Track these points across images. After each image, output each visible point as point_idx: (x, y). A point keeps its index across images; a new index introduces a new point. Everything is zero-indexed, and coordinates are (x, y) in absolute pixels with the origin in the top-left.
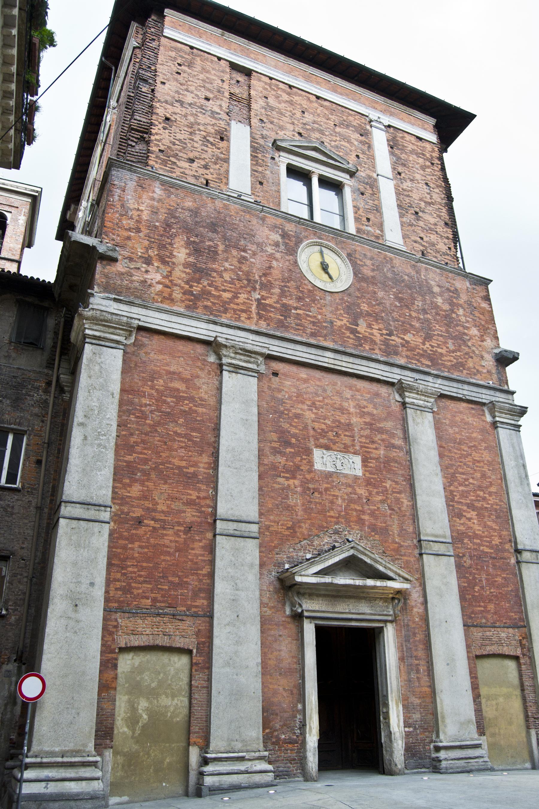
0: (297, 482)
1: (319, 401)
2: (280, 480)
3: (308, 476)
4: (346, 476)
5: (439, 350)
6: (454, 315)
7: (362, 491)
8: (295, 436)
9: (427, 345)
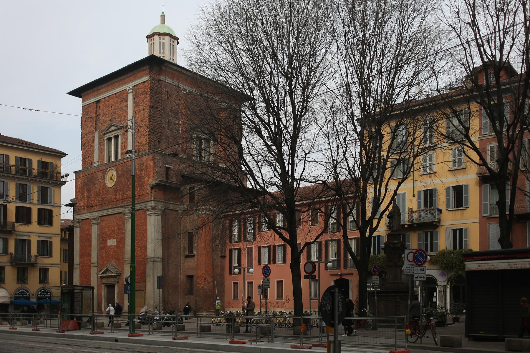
7: (115, 249)
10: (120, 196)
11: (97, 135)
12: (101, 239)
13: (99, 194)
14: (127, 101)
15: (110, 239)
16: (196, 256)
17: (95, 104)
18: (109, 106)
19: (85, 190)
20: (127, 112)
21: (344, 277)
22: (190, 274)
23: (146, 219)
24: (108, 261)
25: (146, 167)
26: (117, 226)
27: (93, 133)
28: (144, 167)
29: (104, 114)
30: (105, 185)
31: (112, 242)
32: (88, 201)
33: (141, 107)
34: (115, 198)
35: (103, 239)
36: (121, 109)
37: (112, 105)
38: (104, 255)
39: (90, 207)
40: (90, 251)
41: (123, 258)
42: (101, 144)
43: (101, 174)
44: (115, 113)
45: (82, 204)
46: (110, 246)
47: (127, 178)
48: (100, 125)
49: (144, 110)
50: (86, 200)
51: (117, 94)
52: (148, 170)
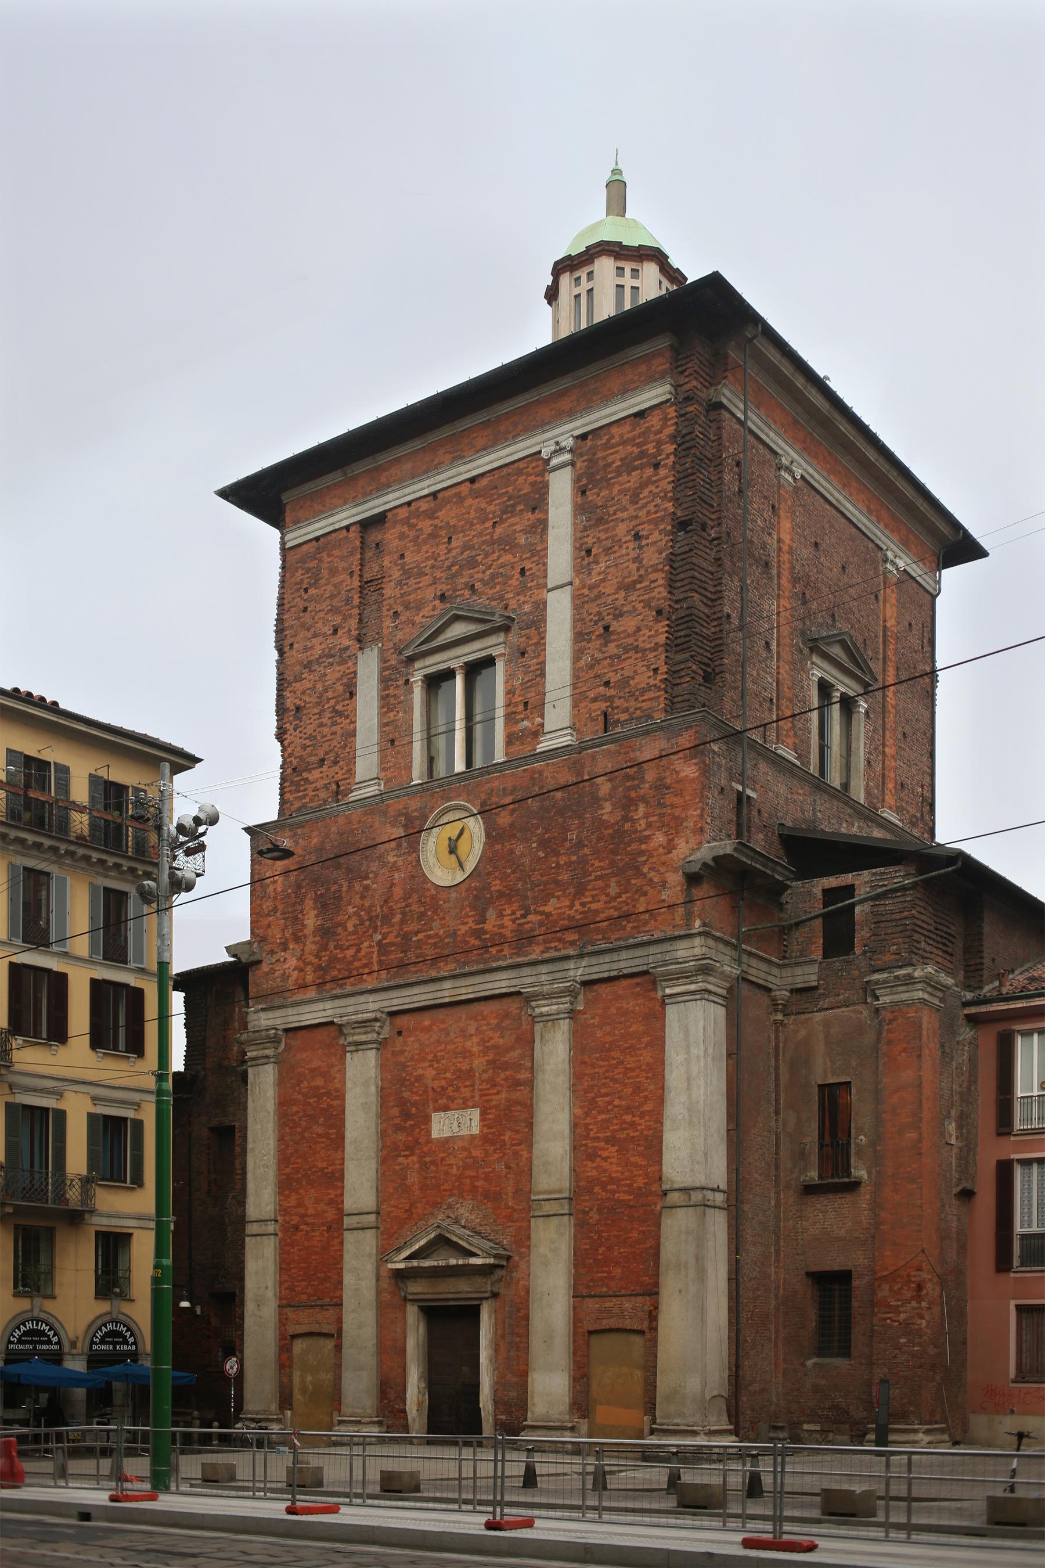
0: (415, 1158)
1: (441, 1051)
2: (401, 1160)
3: (425, 1149)
4: (462, 1138)
5: (594, 906)
6: (628, 826)
7: (477, 1153)
8: (414, 1104)
9: (577, 907)
10: (507, 921)
12: (395, 1112)
15: (446, 1109)
26: (486, 1051)
35: (403, 1112)
46: (447, 1140)
47: (543, 844)
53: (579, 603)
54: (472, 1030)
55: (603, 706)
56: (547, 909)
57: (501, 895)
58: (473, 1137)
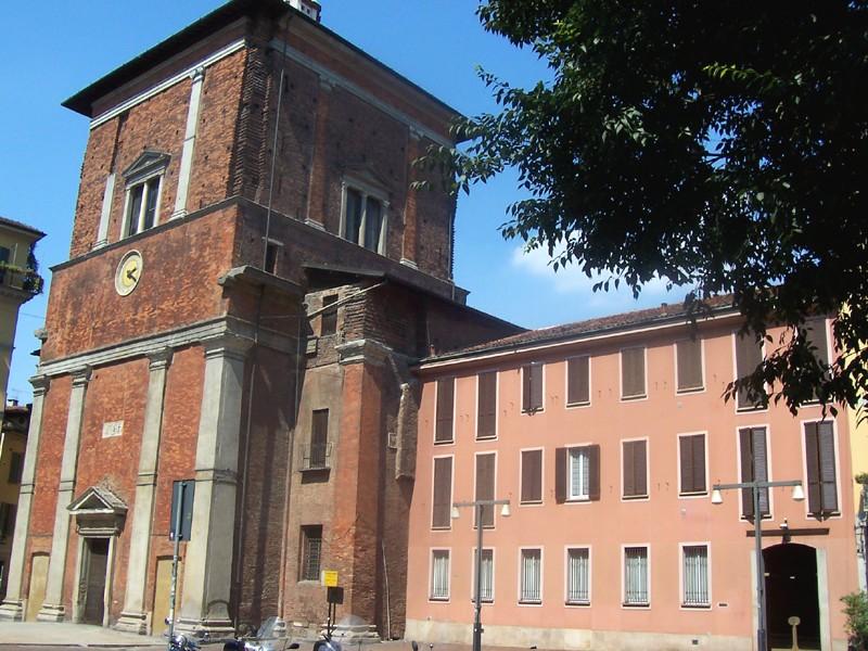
11: (111, 182)
13: (98, 316)
14: (187, 100)
15: (110, 421)
16: (332, 475)
17: (117, 121)
18: (145, 118)
19: (69, 306)
20: (184, 123)
21: (794, 540)
22: (309, 519)
23: (202, 367)
24: (100, 477)
25: (217, 238)
26: (129, 388)
27: (103, 180)
28: (210, 240)
29: (133, 137)
30: (113, 291)
31: (112, 430)
32: (72, 331)
33: (219, 108)
34: (133, 321)
35: (93, 420)
36: (173, 120)
37: (154, 114)
38: (92, 462)
39: (73, 347)
40: (61, 451)
41: (136, 470)
42: (117, 201)
43: (109, 267)
44: (159, 130)
45: (59, 339)
46: (108, 439)
48: (123, 162)
49: (224, 112)
50: (67, 331)
51: (169, 91)
52: (221, 245)
53: (197, 146)
54: (125, 376)
55: (200, 197)
56: (163, 306)
57: (146, 299)
58: (119, 437)
